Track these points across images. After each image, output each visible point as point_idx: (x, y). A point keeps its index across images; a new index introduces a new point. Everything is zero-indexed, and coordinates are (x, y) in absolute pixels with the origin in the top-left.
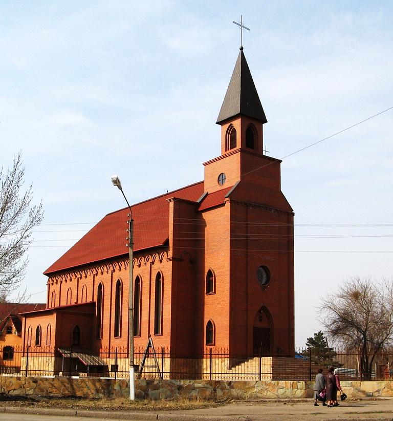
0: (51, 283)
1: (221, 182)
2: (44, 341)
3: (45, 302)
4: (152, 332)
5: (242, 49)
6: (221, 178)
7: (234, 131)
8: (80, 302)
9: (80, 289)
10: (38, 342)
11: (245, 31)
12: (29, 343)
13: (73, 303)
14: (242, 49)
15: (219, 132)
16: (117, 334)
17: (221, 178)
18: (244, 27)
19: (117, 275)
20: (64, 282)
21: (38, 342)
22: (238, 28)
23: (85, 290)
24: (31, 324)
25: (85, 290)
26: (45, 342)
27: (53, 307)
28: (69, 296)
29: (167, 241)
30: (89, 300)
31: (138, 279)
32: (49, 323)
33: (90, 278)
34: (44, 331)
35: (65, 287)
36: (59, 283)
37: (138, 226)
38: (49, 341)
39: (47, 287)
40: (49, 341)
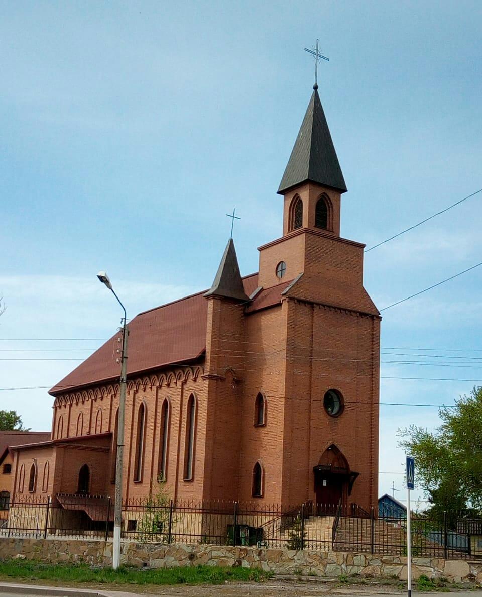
0: (58, 405)
1: (279, 274)
2: (39, 486)
3: (49, 429)
4: (181, 477)
5: (316, 88)
6: (280, 268)
7: (301, 202)
8: (93, 433)
9: (94, 415)
10: (32, 487)
11: (322, 63)
12: (21, 487)
13: (85, 434)
14: (316, 88)
15: (279, 206)
16: (138, 480)
17: (280, 267)
18: (320, 56)
19: (164, 393)
20: (74, 405)
21: (32, 487)
22: (311, 59)
23: (100, 416)
24: (25, 463)
25: (100, 416)
26: (41, 486)
27: (86, 430)
28: (80, 424)
29: (204, 352)
30: (105, 430)
31: (165, 403)
32: (48, 463)
33: (107, 399)
34: (40, 471)
35: (76, 410)
36: (68, 406)
37: (173, 331)
38: (45, 486)
39: (52, 410)
40: (45, 486)
